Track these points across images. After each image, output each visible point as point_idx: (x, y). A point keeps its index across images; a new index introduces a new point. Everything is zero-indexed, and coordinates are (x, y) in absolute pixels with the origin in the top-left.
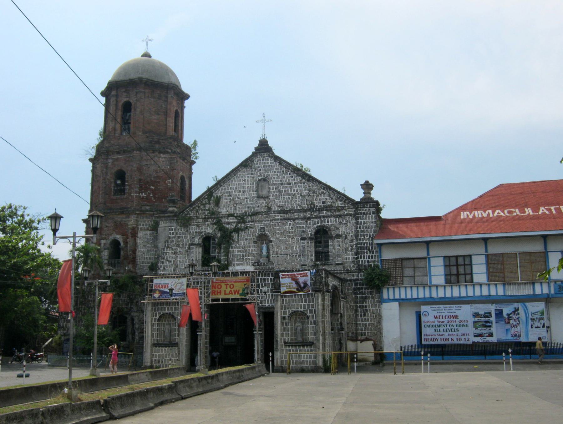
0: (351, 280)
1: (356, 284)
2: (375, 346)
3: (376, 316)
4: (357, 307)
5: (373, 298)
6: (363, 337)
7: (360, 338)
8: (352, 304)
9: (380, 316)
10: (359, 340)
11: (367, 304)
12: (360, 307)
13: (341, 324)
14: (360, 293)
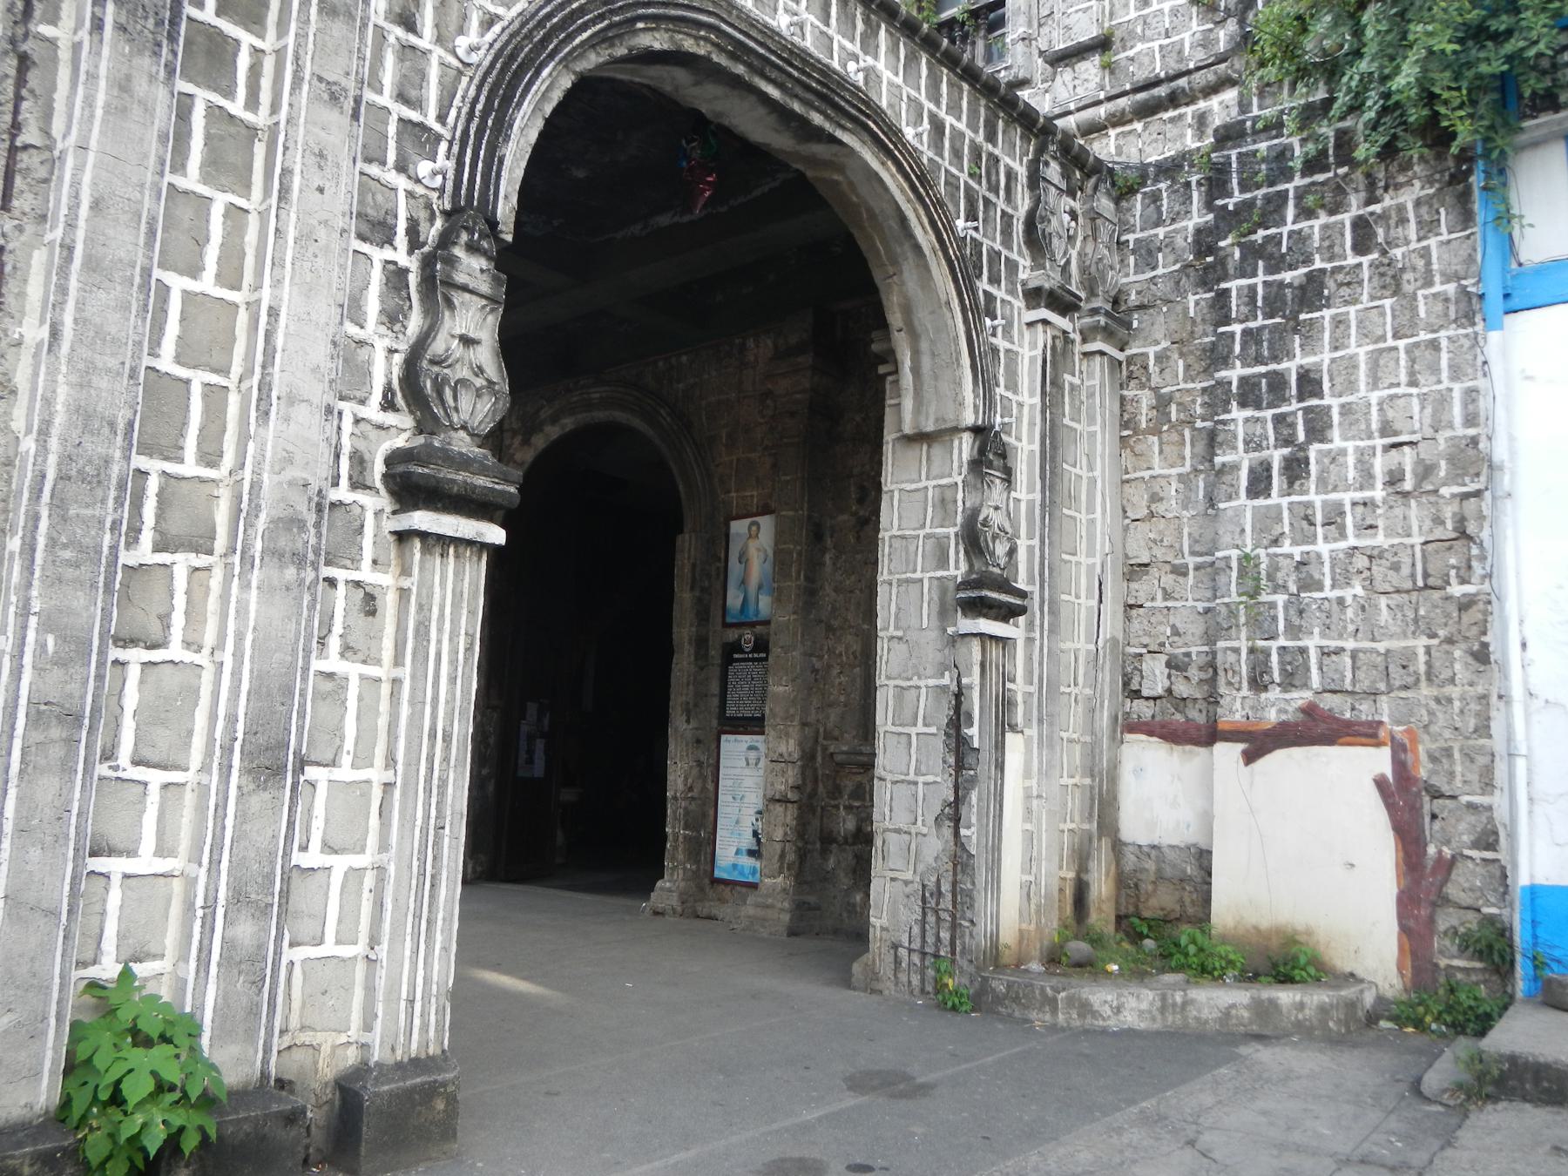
0: (1170, 169)
1: (1216, 183)
2: (1404, 798)
3: (1425, 471)
4: (1218, 398)
5: (1391, 280)
6: (1277, 706)
7: (1236, 707)
8: (1179, 380)
9: (1472, 459)
10: (1233, 736)
11: (1324, 358)
12: (1249, 394)
13: (974, 539)
14: (1253, 253)
